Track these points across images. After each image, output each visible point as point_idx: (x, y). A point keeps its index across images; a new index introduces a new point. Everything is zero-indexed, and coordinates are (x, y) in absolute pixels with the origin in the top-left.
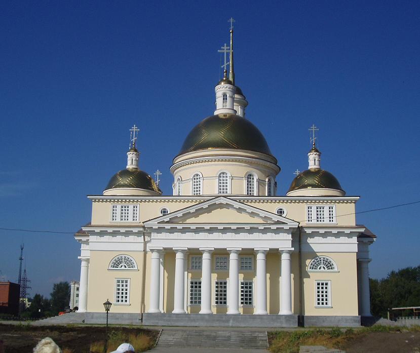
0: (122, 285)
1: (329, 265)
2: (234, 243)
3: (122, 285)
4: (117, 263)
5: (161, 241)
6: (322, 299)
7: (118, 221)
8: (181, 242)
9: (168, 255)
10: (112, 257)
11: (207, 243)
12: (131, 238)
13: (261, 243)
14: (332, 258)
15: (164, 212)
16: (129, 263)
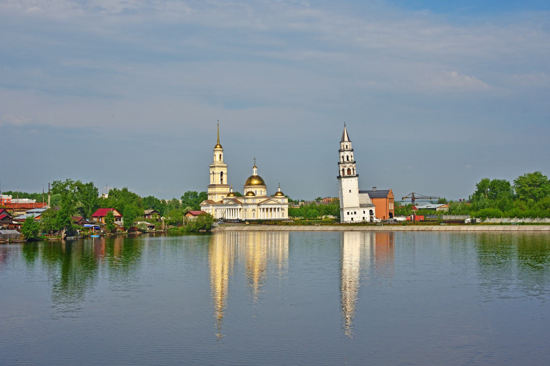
0: (254, 213)
1: (284, 210)
2: (273, 207)
3: (254, 213)
4: (253, 210)
5: (262, 207)
6: (283, 215)
7: (253, 202)
8: (266, 207)
9: (263, 209)
10: (252, 209)
11: (269, 207)
12: (255, 206)
13: (277, 206)
14: (284, 208)
15: (260, 201)
16: (255, 210)
